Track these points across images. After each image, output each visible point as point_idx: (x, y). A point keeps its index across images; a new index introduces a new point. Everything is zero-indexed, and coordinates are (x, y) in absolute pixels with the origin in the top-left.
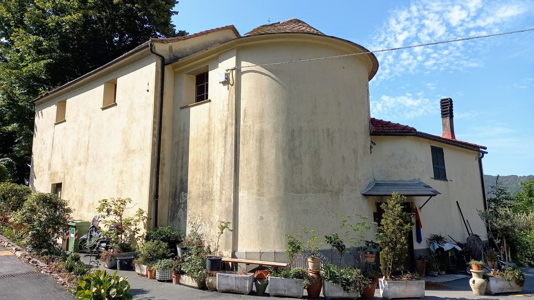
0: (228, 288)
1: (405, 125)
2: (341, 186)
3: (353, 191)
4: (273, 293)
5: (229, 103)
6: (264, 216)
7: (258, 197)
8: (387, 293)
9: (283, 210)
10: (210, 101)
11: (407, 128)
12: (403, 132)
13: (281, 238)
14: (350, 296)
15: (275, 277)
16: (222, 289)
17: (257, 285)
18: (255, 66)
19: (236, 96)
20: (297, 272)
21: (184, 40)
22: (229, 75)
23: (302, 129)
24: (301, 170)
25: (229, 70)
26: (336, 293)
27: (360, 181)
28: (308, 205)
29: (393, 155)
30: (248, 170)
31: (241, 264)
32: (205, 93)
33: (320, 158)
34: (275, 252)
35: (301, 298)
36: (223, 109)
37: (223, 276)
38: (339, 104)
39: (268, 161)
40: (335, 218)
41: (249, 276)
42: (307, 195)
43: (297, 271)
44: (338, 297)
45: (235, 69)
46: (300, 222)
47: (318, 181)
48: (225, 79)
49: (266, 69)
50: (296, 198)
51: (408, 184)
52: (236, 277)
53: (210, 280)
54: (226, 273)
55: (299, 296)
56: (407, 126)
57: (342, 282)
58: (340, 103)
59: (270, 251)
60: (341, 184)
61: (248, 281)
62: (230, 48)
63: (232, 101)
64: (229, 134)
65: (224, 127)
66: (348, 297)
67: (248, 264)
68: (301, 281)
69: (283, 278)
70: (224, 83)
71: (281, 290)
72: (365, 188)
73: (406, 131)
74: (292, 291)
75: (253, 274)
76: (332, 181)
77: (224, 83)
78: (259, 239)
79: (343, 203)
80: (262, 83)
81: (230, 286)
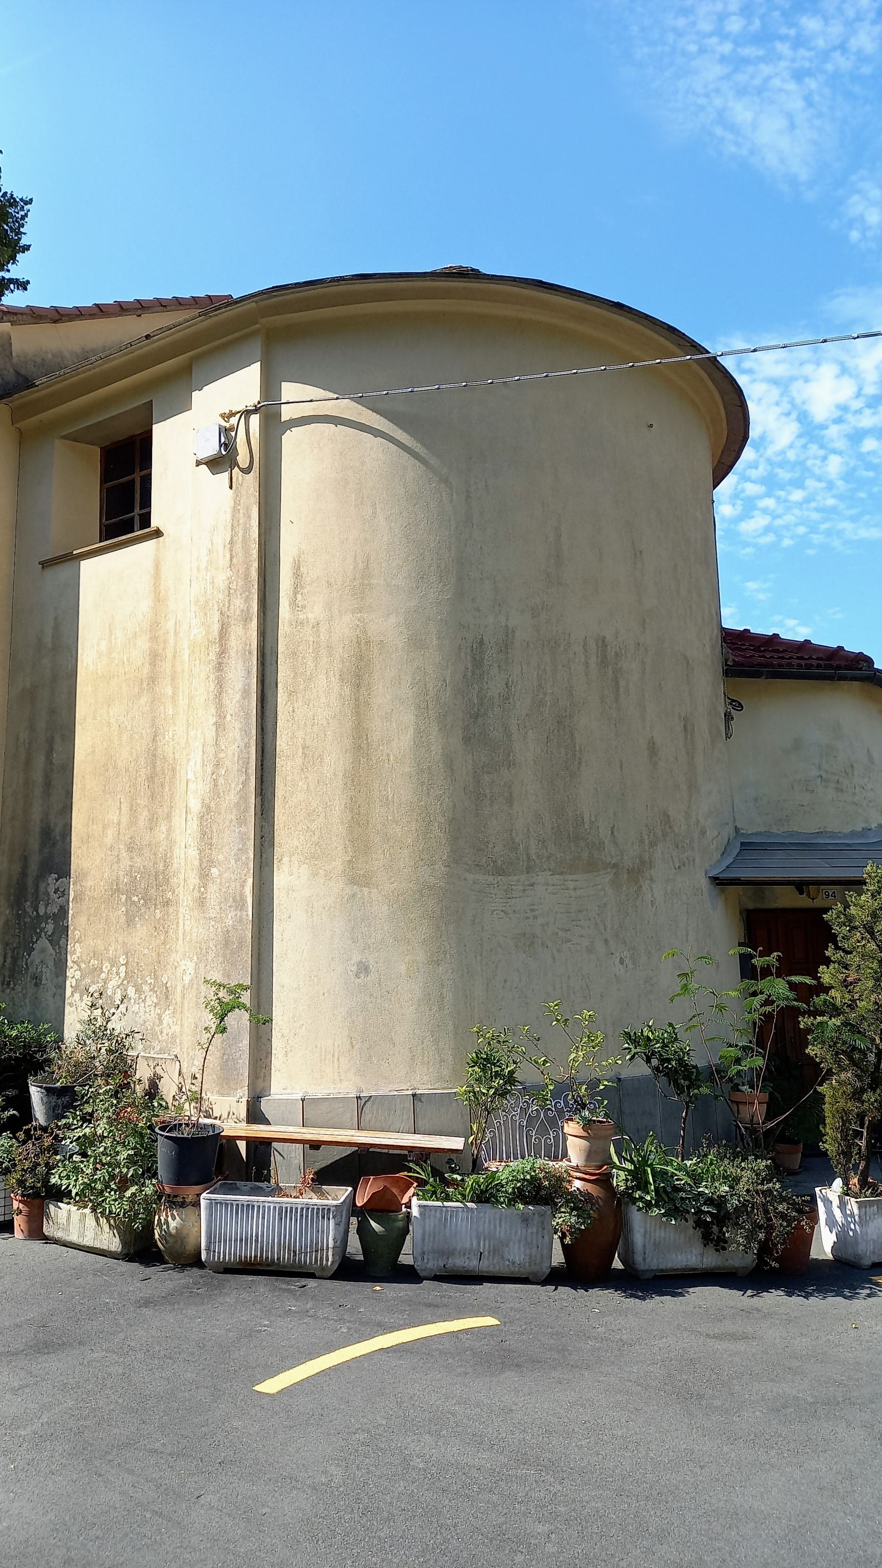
0: (251, 1252)
1: (835, 645)
2: (647, 848)
3: (684, 865)
4: (433, 1264)
5: (235, 538)
6: (371, 961)
7: (348, 891)
8: (857, 1243)
9: (444, 938)
10: (158, 533)
11: (842, 653)
12: (830, 667)
13: (436, 1042)
14: (727, 1264)
15: (439, 1203)
16: (219, 1257)
17: (363, 1231)
18: (337, 399)
19: (263, 510)
20: (527, 1180)
21: (55, 322)
22: (233, 434)
23: (510, 636)
24: (510, 787)
25: (232, 414)
26: (674, 1256)
27: (703, 833)
28: (535, 917)
29: (797, 745)
30: (312, 787)
31: (286, 1148)
32: (137, 511)
33: (575, 747)
34: (414, 1095)
35: (544, 1283)
36: (210, 562)
37: (227, 1204)
38: (635, 555)
39: (388, 755)
40: (631, 966)
41: (335, 1203)
42: (532, 881)
43: (528, 1177)
44: (684, 1270)
45: (256, 410)
46: (505, 981)
47: (571, 830)
48: (220, 446)
49: (377, 413)
50: (492, 891)
51: (848, 845)
52: (284, 1206)
53: (173, 1224)
54: (233, 1190)
55: (535, 1274)
56: (841, 648)
57: (699, 1212)
58: (641, 552)
59: (396, 1093)
60: (647, 842)
61: (332, 1222)
62: (237, 335)
63: (246, 530)
64: (233, 654)
65: (216, 627)
66: (719, 1268)
67: (315, 1145)
68: (542, 1215)
69: (470, 1205)
70: (214, 464)
71: (464, 1253)
72: (717, 856)
73: (843, 663)
74: (506, 1256)
75: (350, 1189)
76: (618, 829)
77: (214, 464)
78: (353, 1047)
79: (654, 907)
80: (363, 463)
81: (256, 1247)
